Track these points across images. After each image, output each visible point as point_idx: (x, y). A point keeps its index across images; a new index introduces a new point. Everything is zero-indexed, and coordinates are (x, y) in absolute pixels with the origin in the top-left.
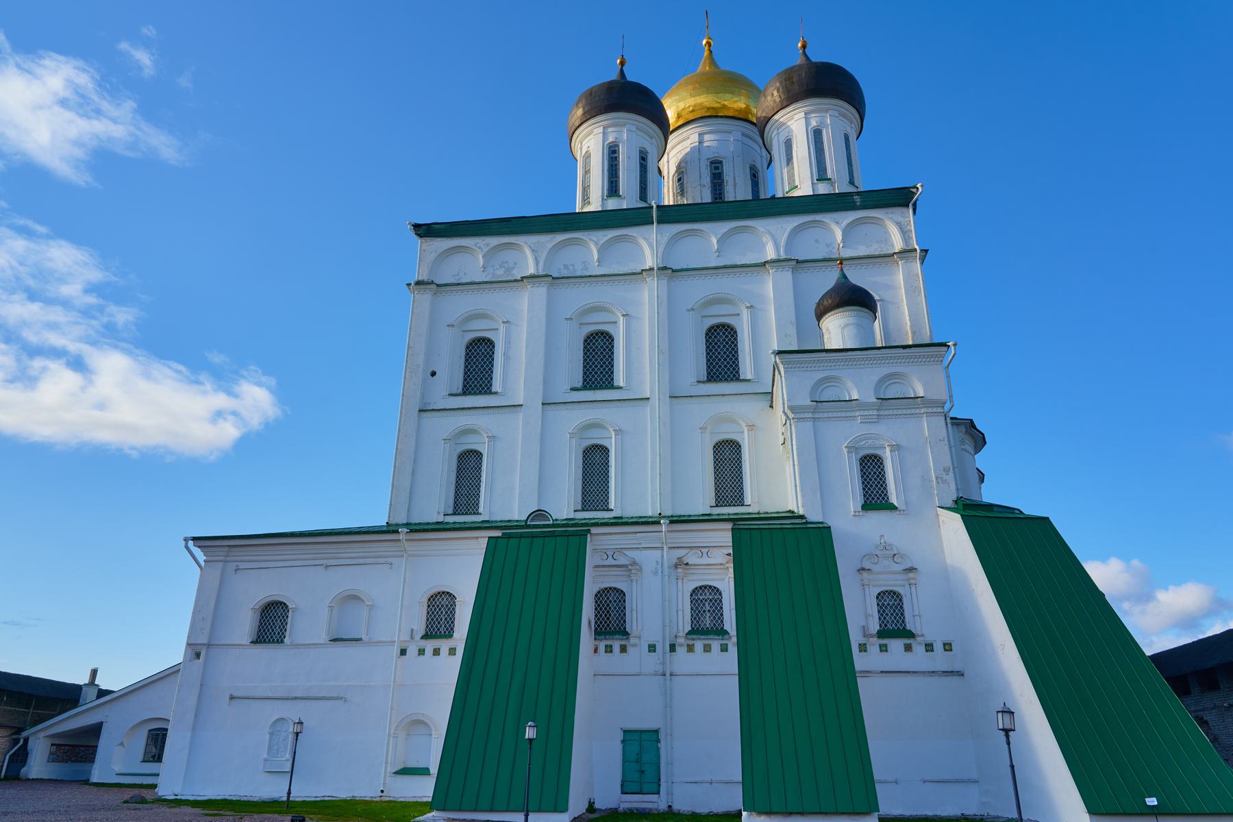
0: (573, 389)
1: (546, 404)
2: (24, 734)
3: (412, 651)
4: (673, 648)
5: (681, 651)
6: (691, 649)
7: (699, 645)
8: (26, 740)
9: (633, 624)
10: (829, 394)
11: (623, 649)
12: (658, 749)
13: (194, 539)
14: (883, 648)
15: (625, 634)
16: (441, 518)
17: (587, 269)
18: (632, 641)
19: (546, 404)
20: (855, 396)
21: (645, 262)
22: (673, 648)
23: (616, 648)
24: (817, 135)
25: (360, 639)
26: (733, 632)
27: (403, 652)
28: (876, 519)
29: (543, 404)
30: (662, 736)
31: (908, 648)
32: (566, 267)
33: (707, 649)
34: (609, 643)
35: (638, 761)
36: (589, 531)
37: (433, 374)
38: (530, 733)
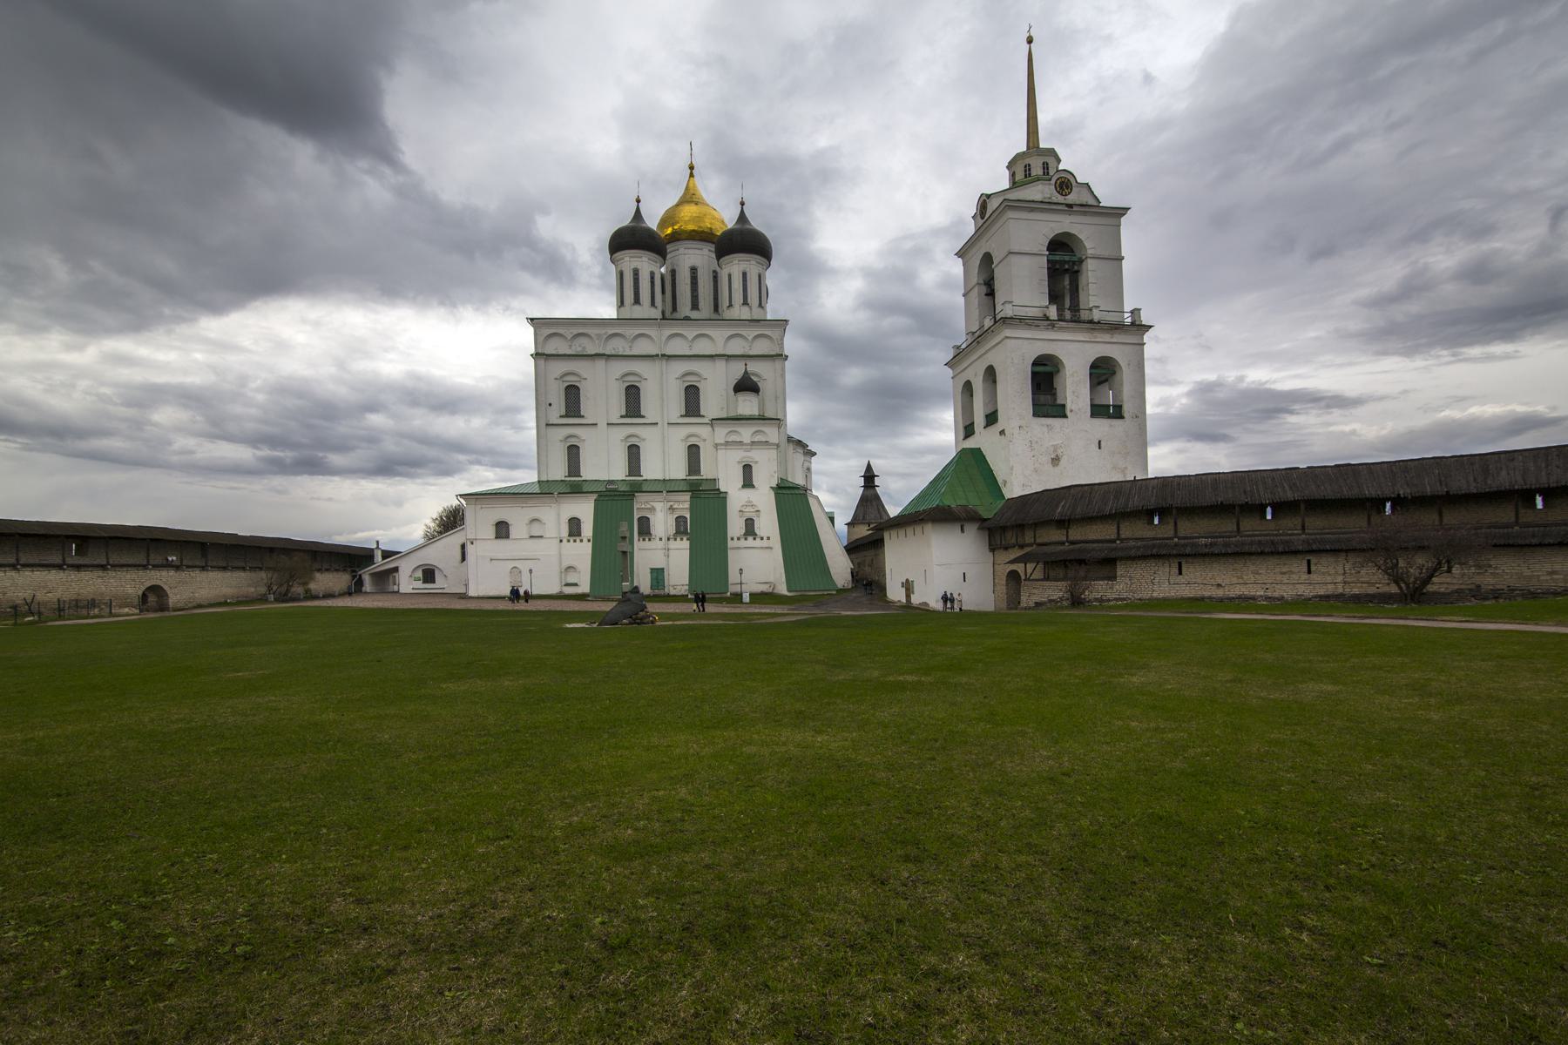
2: (360, 573)
3: (565, 541)
4: (668, 539)
5: (672, 541)
6: (675, 540)
8: (360, 575)
11: (650, 540)
15: (651, 534)
16: (563, 479)
17: (624, 351)
22: (668, 539)
23: (647, 539)
24: (744, 274)
25: (541, 537)
27: (561, 541)
29: (608, 424)
31: (755, 539)
33: (682, 539)
35: (657, 579)
37: (550, 405)
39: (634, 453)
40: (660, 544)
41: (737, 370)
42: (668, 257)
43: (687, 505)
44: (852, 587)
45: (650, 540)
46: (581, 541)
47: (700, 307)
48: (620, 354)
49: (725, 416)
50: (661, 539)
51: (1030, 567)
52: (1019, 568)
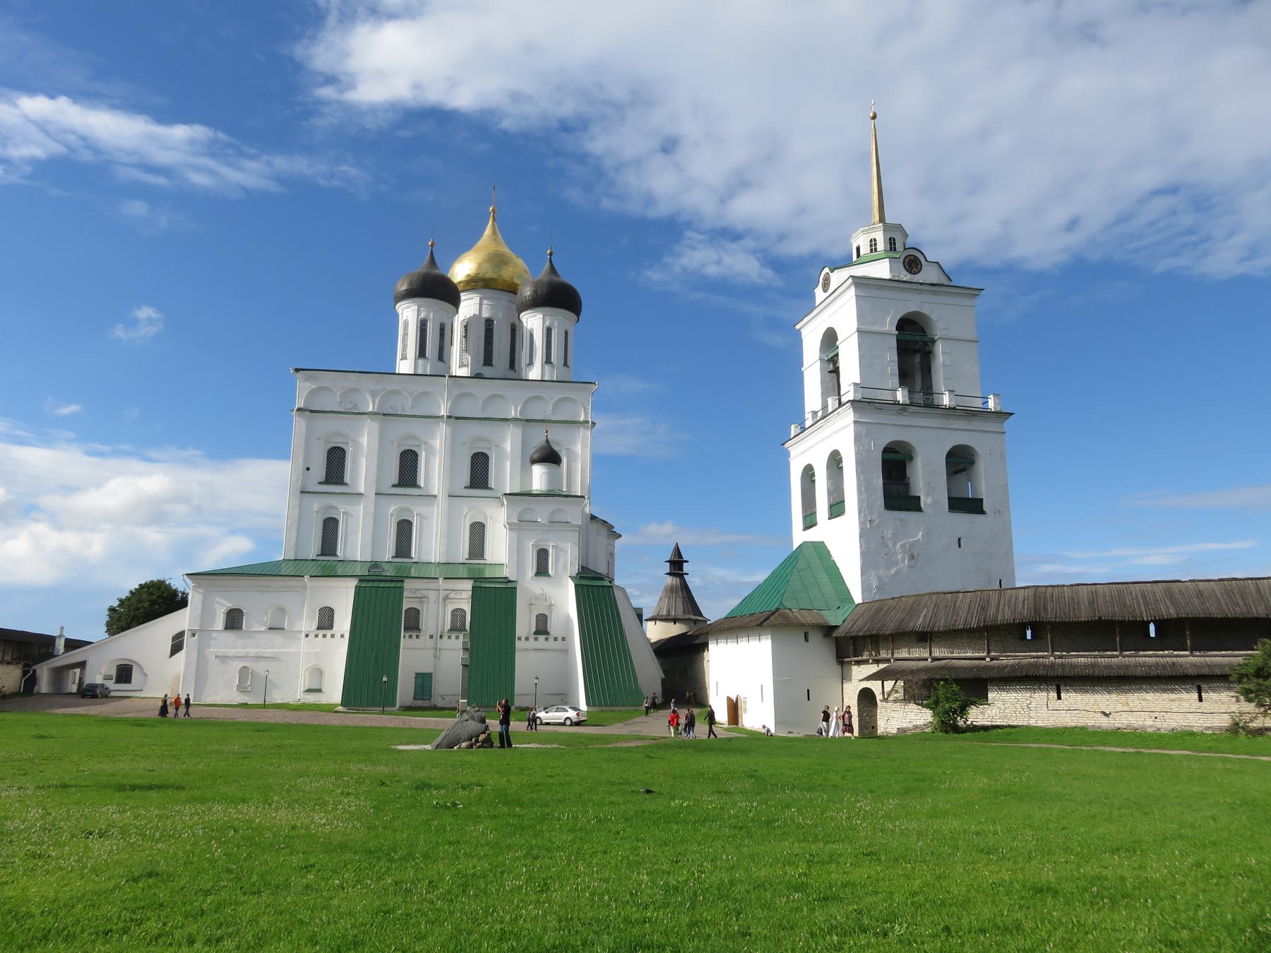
0: (394, 486)
1: (379, 494)
2: (34, 668)
3: (312, 636)
5: (445, 638)
6: (449, 637)
7: (453, 636)
8: (35, 671)
9: (423, 625)
10: (527, 517)
11: (417, 637)
12: (431, 681)
13: (187, 574)
14: (536, 639)
15: (418, 629)
17: (403, 410)
18: (422, 633)
19: (379, 494)
20: (539, 520)
21: (440, 412)
22: (441, 637)
23: (414, 636)
26: (468, 630)
27: (307, 636)
28: (542, 579)
30: (433, 675)
31: (547, 639)
32: (391, 407)
34: (410, 634)
36: (403, 581)
37: (308, 469)
38: (385, 679)
39: (404, 529)
40: (430, 643)
41: (538, 438)
42: (462, 305)
43: (468, 595)
44: (663, 702)
45: (417, 637)
46: (333, 636)
47: (493, 363)
48: (399, 413)
49: (517, 490)
50: (431, 637)
51: (889, 685)
52: (875, 686)
